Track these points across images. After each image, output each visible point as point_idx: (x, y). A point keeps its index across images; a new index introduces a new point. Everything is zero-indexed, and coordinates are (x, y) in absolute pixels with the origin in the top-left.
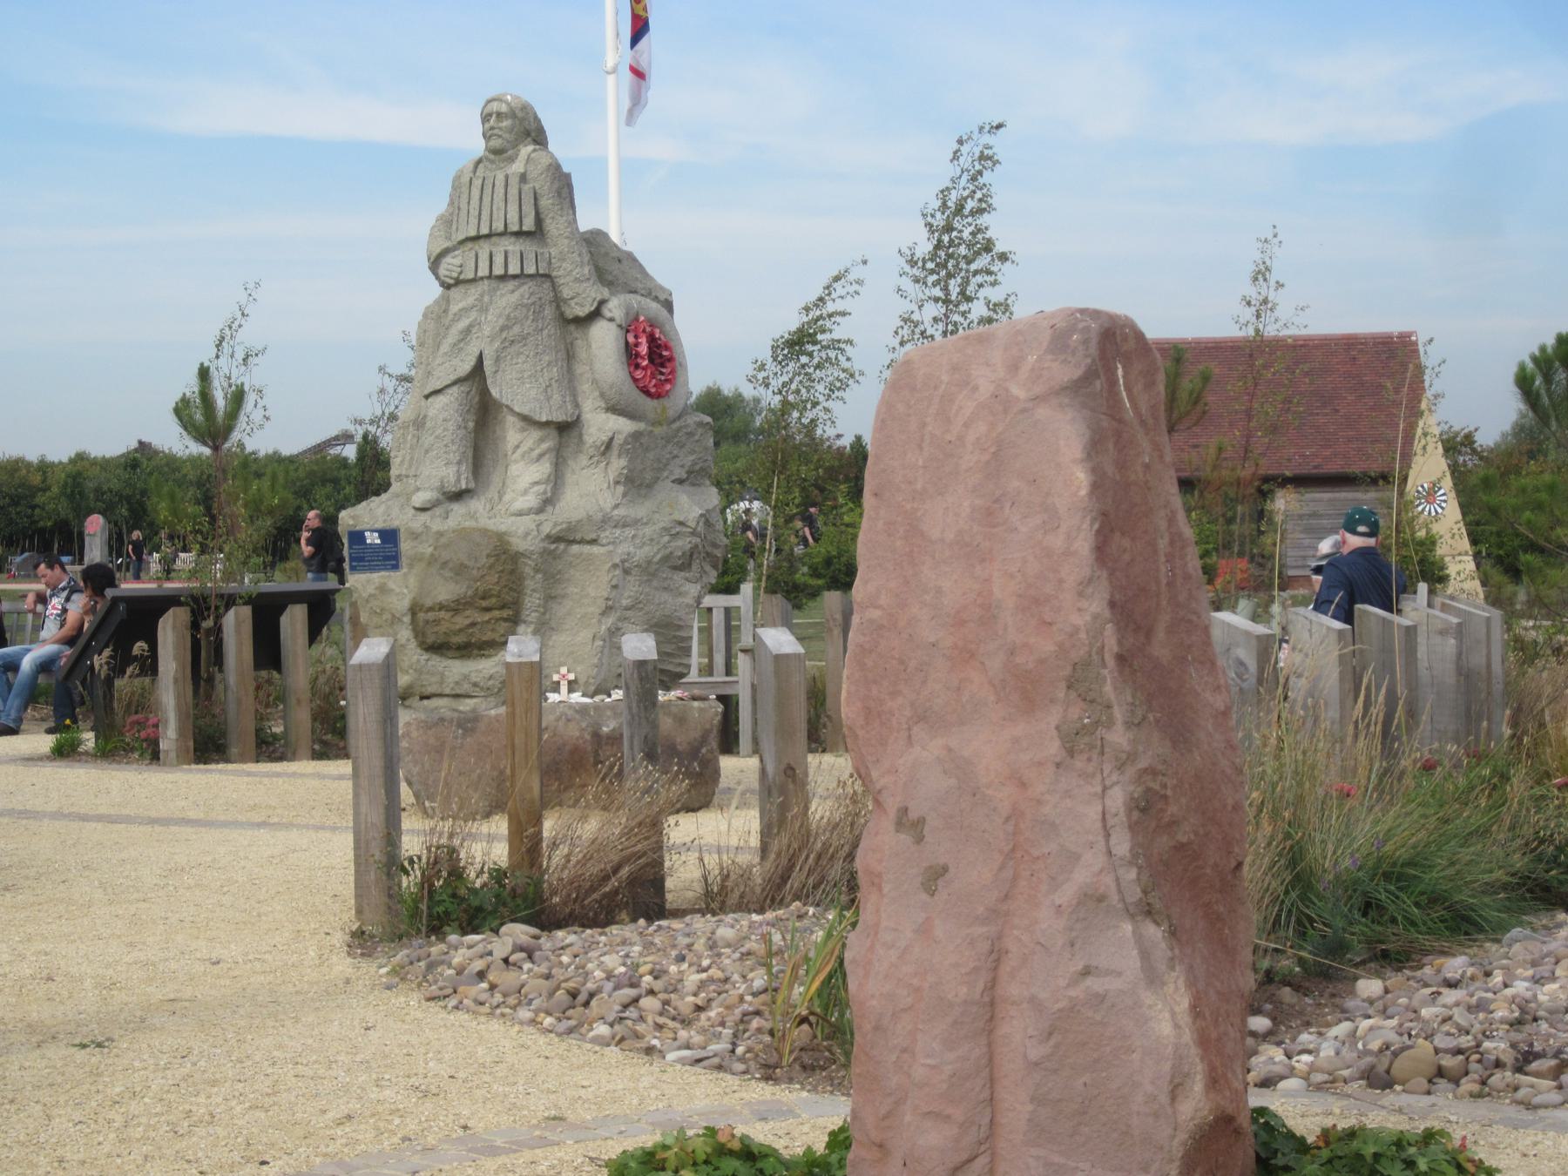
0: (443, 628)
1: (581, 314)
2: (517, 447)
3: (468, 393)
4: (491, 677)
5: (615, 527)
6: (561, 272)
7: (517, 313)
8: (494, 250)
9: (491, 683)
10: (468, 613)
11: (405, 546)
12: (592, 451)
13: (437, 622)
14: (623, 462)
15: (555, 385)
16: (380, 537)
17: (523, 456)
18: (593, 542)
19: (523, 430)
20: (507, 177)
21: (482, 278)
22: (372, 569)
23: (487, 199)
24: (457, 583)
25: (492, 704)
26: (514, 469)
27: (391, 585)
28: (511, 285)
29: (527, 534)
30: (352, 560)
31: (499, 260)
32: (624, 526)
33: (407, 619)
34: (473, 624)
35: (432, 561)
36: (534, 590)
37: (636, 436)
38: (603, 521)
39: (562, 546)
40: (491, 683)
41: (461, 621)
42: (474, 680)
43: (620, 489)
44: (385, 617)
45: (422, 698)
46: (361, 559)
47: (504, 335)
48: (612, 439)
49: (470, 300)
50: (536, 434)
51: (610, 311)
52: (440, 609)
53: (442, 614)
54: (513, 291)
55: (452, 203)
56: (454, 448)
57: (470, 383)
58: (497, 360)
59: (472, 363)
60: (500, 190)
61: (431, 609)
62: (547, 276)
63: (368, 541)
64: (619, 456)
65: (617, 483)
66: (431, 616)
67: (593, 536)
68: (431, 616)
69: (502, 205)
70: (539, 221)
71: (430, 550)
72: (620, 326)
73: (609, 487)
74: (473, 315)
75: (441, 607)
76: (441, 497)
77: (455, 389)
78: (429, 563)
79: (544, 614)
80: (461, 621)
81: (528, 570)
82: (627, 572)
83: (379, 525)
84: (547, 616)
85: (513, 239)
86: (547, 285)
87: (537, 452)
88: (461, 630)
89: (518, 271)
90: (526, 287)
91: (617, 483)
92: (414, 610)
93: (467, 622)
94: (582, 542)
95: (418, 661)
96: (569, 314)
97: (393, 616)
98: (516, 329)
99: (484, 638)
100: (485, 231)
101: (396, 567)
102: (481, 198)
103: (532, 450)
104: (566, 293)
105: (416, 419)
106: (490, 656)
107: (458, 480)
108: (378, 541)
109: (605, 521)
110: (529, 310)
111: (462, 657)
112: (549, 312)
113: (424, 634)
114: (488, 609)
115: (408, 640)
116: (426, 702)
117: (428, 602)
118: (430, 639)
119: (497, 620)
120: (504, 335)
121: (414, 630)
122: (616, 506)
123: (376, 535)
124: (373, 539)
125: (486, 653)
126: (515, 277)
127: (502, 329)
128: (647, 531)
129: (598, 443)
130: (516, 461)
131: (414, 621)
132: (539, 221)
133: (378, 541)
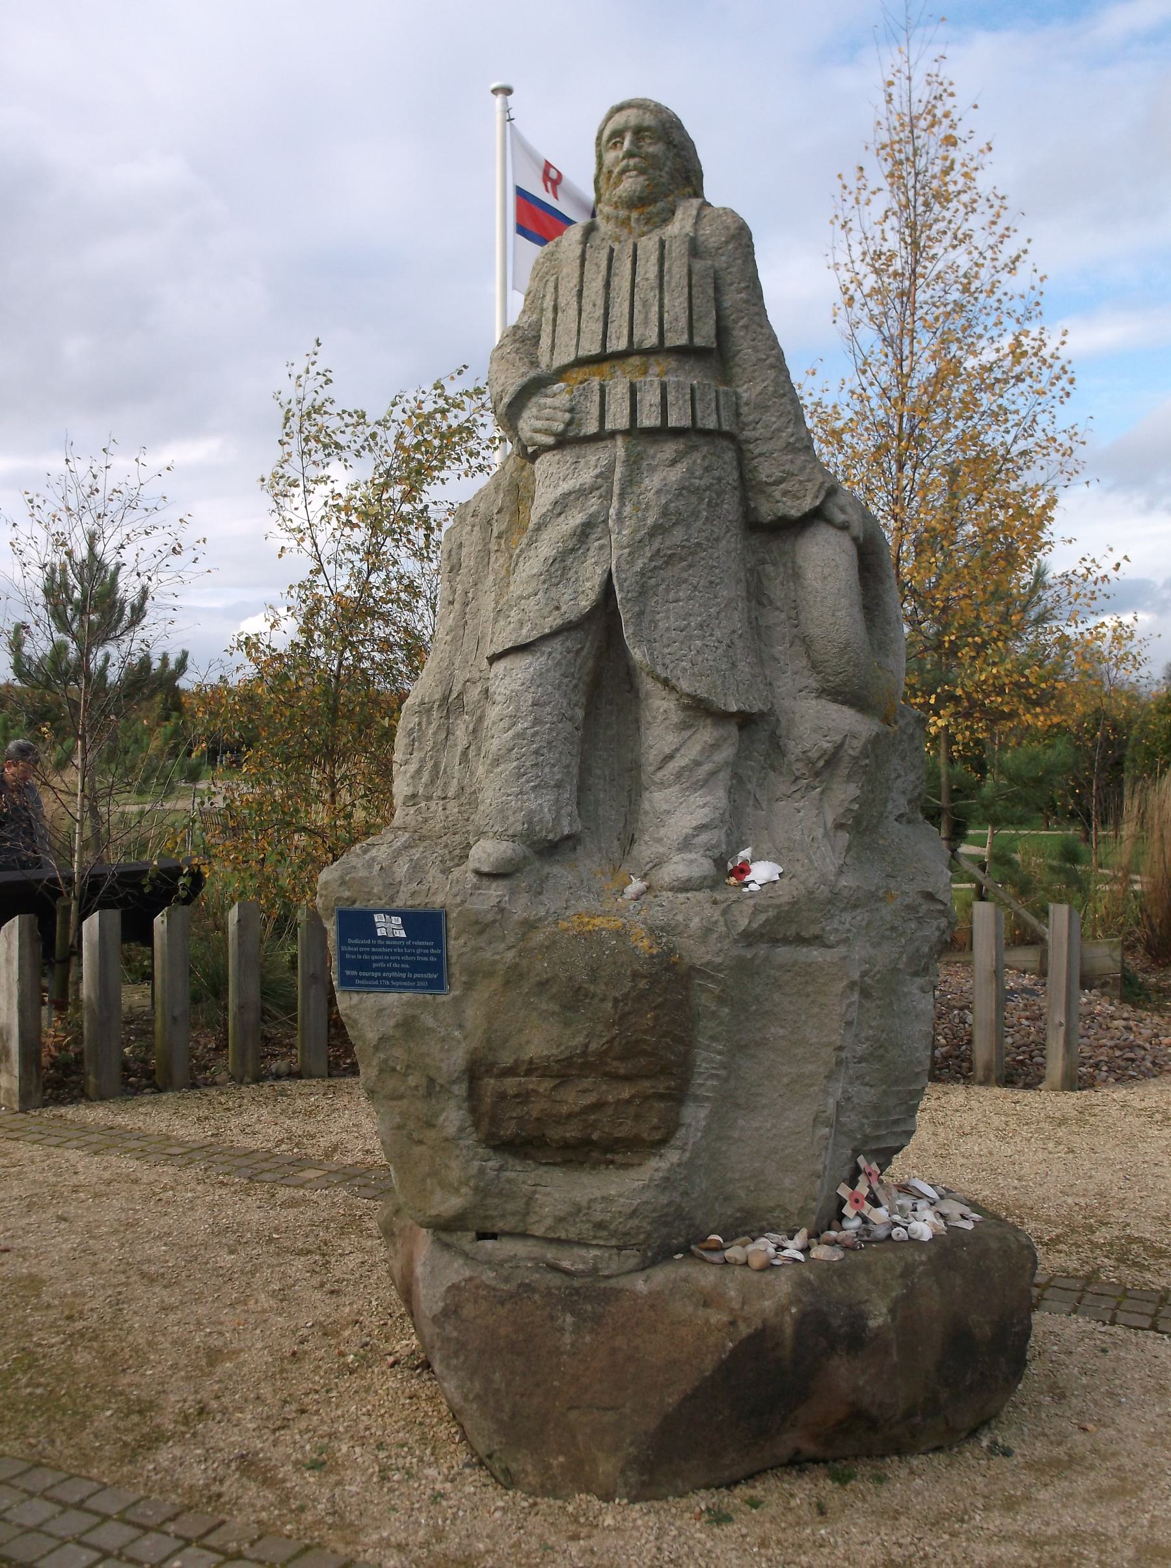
0: (536, 1108)
1: (795, 513)
2: (670, 757)
3: (578, 652)
4: (634, 1214)
5: (844, 910)
6: (760, 431)
7: (680, 503)
8: (639, 380)
9: (635, 1222)
10: (586, 1083)
11: (456, 945)
12: (799, 768)
13: (524, 1097)
14: (853, 790)
15: (739, 644)
16: (405, 925)
17: (679, 775)
18: (817, 940)
19: (683, 726)
20: (662, 244)
21: (613, 434)
22: (386, 985)
23: (622, 283)
24: (567, 1024)
25: (632, 1262)
26: (657, 799)
27: (428, 1021)
28: (669, 449)
29: (708, 931)
30: (344, 963)
31: (650, 398)
32: (855, 907)
33: (460, 1089)
34: (598, 1106)
35: (514, 977)
36: (713, 1038)
37: (876, 740)
38: (830, 902)
39: (762, 950)
40: (635, 1222)
41: (573, 1098)
42: (598, 1217)
43: (844, 837)
44: (412, 1081)
45: (482, 1236)
46: (364, 965)
47: (656, 545)
48: (839, 747)
49: (586, 476)
50: (706, 734)
51: (843, 510)
52: (528, 1073)
53: (532, 1082)
54: (673, 463)
55: (533, 300)
56: (551, 756)
57: (580, 634)
58: (643, 592)
59: (593, 596)
60: (649, 269)
61: (510, 1072)
62: (730, 436)
64: (849, 778)
65: (839, 826)
66: (511, 1084)
67: (815, 930)
68: (511, 1084)
69: (653, 296)
70: (722, 331)
71: (510, 955)
72: (855, 539)
73: (826, 835)
74: (593, 504)
75: (531, 1069)
76: (528, 852)
77: (557, 645)
78: (507, 983)
79: (726, 1080)
80: (573, 1098)
81: (705, 1001)
82: (865, 994)
83: (402, 900)
84: (732, 1083)
85: (673, 363)
86: (729, 456)
87: (707, 767)
88: (570, 1116)
89: (686, 422)
90: (697, 457)
91: (839, 826)
92: (475, 1072)
93: (591, 1099)
94: (800, 940)
95: (482, 1171)
96: (766, 511)
97: (431, 1080)
98: (678, 535)
99: (622, 1132)
100: (618, 344)
101: (437, 985)
102: (607, 285)
103: (697, 764)
104: (766, 471)
105: (445, 698)
106: (626, 1166)
107: (557, 819)
108: (403, 934)
109: (834, 901)
110: (701, 499)
111: (566, 1163)
112: (730, 506)
113: (495, 1120)
114: (628, 1078)
115: (461, 1129)
116: (489, 1244)
117: (506, 1059)
118: (509, 1130)
119: (646, 1098)
120: (656, 545)
121: (473, 1110)
122: (840, 872)
123: (397, 920)
124: (389, 927)
125: (619, 1158)
126: (678, 433)
127: (656, 530)
128: (886, 912)
129: (814, 754)
130: (663, 785)
131: (473, 1095)
132: (722, 331)
133: (403, 934)
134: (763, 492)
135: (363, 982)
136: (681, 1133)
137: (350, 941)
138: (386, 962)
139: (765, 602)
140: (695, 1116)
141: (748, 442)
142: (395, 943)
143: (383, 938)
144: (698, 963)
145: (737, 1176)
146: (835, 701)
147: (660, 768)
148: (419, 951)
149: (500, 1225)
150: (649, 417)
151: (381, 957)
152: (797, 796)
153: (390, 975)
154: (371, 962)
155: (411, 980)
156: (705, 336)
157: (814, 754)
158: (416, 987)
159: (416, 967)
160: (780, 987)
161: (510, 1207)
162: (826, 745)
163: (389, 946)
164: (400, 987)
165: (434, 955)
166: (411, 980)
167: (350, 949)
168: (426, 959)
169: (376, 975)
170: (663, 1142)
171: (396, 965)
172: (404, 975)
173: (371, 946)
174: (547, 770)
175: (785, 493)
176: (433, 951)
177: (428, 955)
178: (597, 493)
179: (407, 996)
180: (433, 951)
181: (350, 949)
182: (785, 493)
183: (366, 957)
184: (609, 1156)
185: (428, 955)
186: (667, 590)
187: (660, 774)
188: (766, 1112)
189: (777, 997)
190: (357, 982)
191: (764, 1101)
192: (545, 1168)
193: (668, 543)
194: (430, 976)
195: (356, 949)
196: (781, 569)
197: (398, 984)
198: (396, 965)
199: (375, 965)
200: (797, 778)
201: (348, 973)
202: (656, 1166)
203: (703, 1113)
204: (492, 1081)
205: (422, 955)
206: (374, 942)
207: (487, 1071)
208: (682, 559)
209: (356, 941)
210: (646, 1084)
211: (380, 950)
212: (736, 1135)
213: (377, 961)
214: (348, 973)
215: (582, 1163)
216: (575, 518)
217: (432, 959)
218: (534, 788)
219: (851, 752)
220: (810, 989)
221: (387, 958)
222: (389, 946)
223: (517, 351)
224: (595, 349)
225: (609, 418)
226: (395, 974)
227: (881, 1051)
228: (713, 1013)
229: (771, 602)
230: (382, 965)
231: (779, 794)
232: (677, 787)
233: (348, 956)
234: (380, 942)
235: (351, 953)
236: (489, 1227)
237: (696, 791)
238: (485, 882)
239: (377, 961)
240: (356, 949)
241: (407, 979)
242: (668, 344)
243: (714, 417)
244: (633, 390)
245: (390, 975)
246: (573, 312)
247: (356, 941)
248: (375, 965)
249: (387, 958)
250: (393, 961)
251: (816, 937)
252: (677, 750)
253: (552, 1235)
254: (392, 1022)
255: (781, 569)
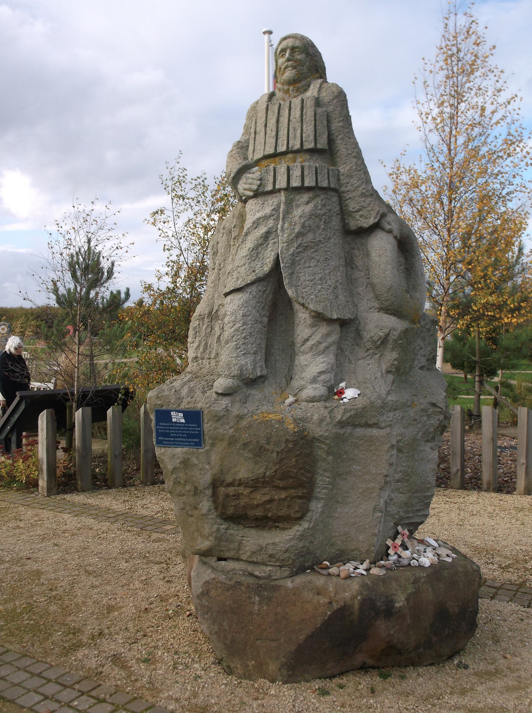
0: (243, 502)
1: (366, 225)
2: (307, 340)
3: (264, 291)
4: (287, 551)
5: (390, 411)
6: (349, 187)
7: (311, 222)
8: (291, 165)
9: (287, 555)
10: (265, 490)
11: (207, 426)
12: (368, 345)
13: (237, 496)
14: (395, 355)
15: (340, 287)
16: (184, 417)
17: (311, 348)
18: (376, 425)
19: (313, 325)
20: (303, 101)
21: (279, 190)
22: (176, 444)
23: (284, 120)
24: (256, 463)
25: (287, 573)
26: (302, 359)
27: (195, 460)
28: (305, 197)
29: (321, 421)
30: (158, 434)
31: (296, 173)
32: (395, 410)
33: (209, 492)
34: (271, 501)
35: (232, 441)
36: (325, 470)
37: (406, 332)
38: (382, 407)
39: (349, 430)
40: (287, 555)
41: (260, 497)
42: (270, 552)
43: (391, 377)
44: (188, 487)
45: (220, 559)
46: (167, 435)
47: (299, 241)
48: (387, 335)
49: (268, 210)
50: (324, 329)
51: (389, 224)
52: (239, 485)
53: (241, 490)
54: (308, 203)
55: (247, 128)
56: (252, 340)
57: (265, 283)
58: (293, 263)
59: (270, 266)
60: (296, 113)
62: (335, 190)
63: (174, 420)
64: (392, 350)
65: (389, 372)
66: (231, 490)
67: (374, 420)
68: (231, 490)
70: (331, 141)
72: (395, 237)
73: (382, 375)
74: (271, 223)
76: (240, 384)
77: (254, 288)
78: (230, 444)
79: (332, 490)
80: (260, 497)
81: (320, 453)
82: (400, 450)
83: (184, 406)
84: (335, 491)
85: (307, 156)
86: (335, 199)
87: (324, 345)
88: (258, 505)
89: (313, 184)
90: (318, 200)
91: (389, 372)
92: (215, 484)
93: (267, 498)
94: (367, 425)
95: (218, 530)
96: (353, 225)
97: (196, 488)
98: (310, 237)
99: (281, 514)
100: (282, 148)
101: (198, 444)
102: (278, 121)
103: (319, 343)
104: (352, 206)
105: (210, 313)
106: (284, 529)
107: (254, 368)
108: (183, 421)
109: (384, 407)
110: (321, 220)
111: (257, 527)
112: (336, 222)
113: (224, 506)
114: (284, 488)
115: (209, 510)
116: (223, 563)
117: (229, 479)
118: (230, 511)
120: (299, 241)
121: (215, 502)
122: (388, 393)
123: (181, 415)
124: (178, 418)
125: (281, 525)
126: (309, 189)
127: (299, 235)
128: (411, 412)
130: (304, 353)
131: (214, 495)
132: (331, 141)
133: (183, 421)
134: (351, 216)
135: (167, 443)
136: (310, 514)
137: (161, 424)
138: (177, 433)
139: (354, 267)
140: (316, 506)
141: (343, 192)
142: (180, 425)
143: (175, 423)
144: (317, 436)
145: (337, 534)
146: (387, 313)
147: (303, 345)
148: (191, 429)
149: (227, 555)
150: (295, 182)
151: (174, 431)
152: (368, 358)
153: (178, 439)
154: (169, 433)
155: (188, 442)
156: (322, 143)
157: (376, 338)
158: (189, 445)
159: (190, 436)
160: (358, 447)
161: (231, 546)
162: (381, 334)
163: (178, 426)
164: (183, 445)
165: (197, 431)
166: (188, 442)
167: (161, 427)
168: (194, 432)
169: (172, 439)
170: (301, 518)
171: (181, 435)
172: (184, 440)
173: (170, 426)
174: (249, 346)
175: (361, 216)
176: (197, 429)
177: (195, 431)
178: (272, 218)
179: (185, 449)
180: (197, 429)
181: (161, 427)
182: (361, 216)
183: (168, 431)
184: (277, 524)
185: (195, 431)
186: (305, 262)
187: (303, 348)
188: (351, 505)
189: (356, 452)
190: (164, 442)
191: (350, 500)
192: (248, 529)
193: (305, 241)
194: (195, 440)
195: (163, 428)
196: (361, 252)
197: (181, 443)
198: (181, 435)
199: (171, 435)
200: (368, 349)
201: (160, 438)
202: (297, 529)
203: (320, 505)
204: (223, 489)
205: (192, 430)
206: (171, 424)
207: (221, 484)
208: (312, 248)
209: (163, 424)
210: (292, 491)
211: (174, 428)
212: (337, 515)
213: (173, 433)
214: (160, 438)
215: (264, 527)
216: (263, 230)
217: (197, 432)
218: (244, 354)
219: (393, 337)
220: (372, 448)
221: (177, 432)
222: (178, 426)
223: (238, 153)
224: (271, 151)
225: (277, 183)
226: (180, 439)
227: (407, 478)
228: (325, 459)
229: (357, 267)
230: (175, 435)
231: (360, 357)
232: (310, 354)
233: (160, 431)
234: (174, 424)
235: (161, 429)
236: (222, 555)
237: (319, 355)
238: (220, 397)
239: (173, 433)
240: (163, 428)
241: (185, 442)
242: (305, 147)
243: (327, 181)
244: (288, 169)
245: (178, 439)
246: (262, 134)
247: (163, 424)
248: (171, 435)
249: (177, 432)
250: (180, 433)
251: (375, 424)
252: (310, 336)
253: (250, 560)
254: (178, 461)
255: (361, 252)
